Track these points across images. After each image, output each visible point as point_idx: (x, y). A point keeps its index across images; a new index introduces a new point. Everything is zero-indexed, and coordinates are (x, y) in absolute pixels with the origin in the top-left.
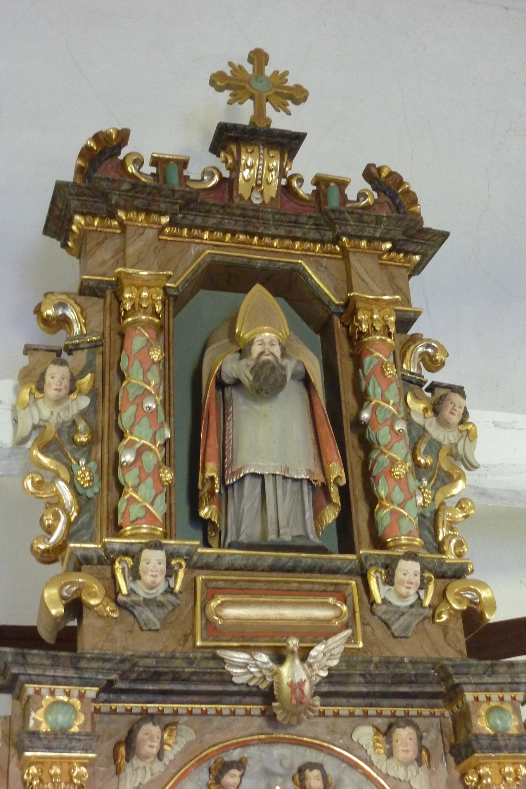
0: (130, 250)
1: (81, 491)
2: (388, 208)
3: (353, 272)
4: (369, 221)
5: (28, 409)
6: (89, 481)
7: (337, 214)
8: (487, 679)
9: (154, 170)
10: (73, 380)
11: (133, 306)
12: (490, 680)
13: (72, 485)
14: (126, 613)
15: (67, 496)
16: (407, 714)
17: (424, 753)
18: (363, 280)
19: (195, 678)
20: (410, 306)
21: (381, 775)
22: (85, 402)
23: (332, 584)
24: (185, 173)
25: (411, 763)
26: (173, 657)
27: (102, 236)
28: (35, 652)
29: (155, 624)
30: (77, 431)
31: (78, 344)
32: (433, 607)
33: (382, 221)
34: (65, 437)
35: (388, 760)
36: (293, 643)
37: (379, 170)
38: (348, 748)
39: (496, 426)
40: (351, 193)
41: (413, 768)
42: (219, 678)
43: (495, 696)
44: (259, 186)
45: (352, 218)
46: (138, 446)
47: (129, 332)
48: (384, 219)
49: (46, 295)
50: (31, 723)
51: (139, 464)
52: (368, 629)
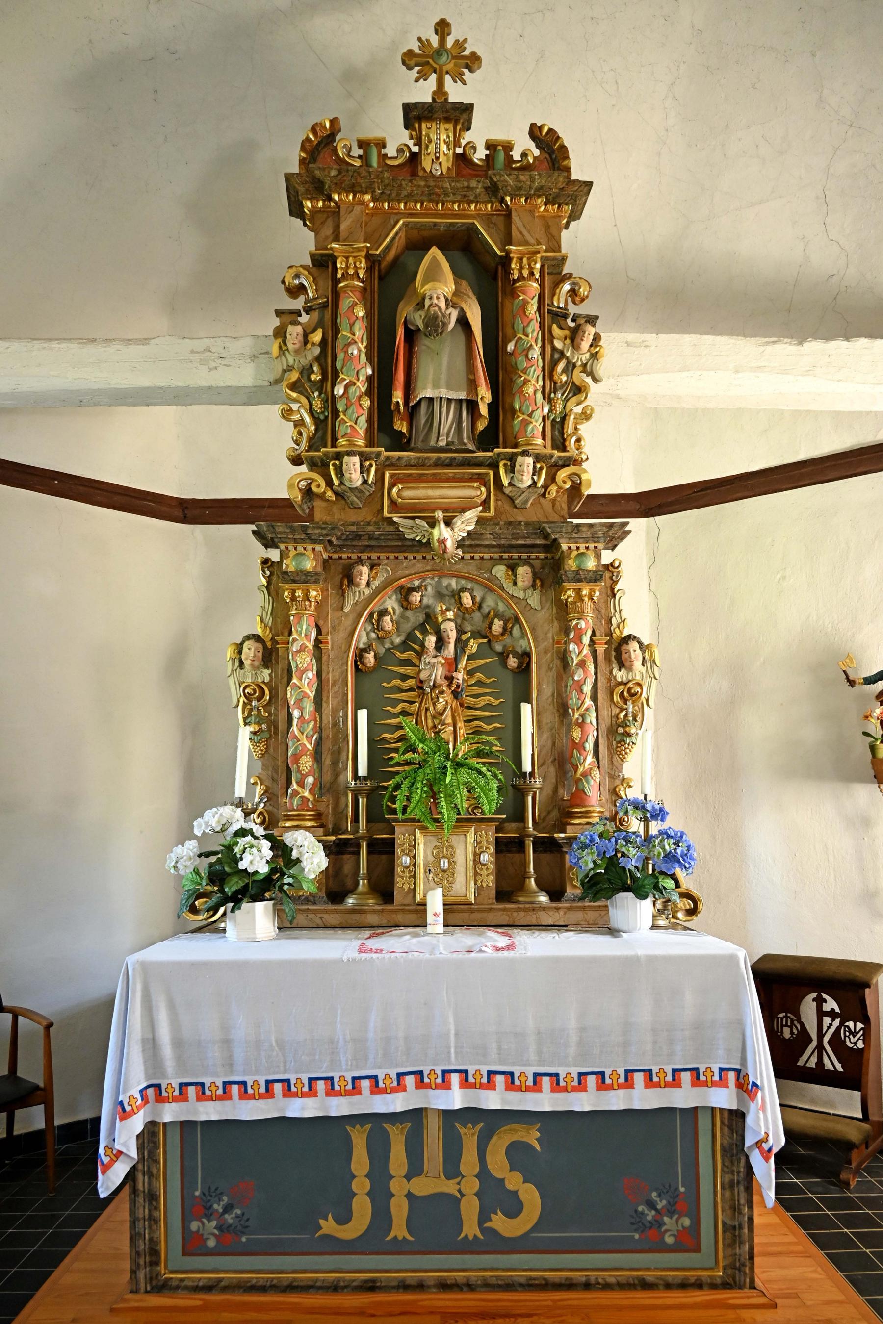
0: (343, 226)
1: (316, 415)
2: (546, 164)
3: (513, 226)
4: (524, 179)
5: (279, 359)
6: (321, 408)
7: (498, 177)
8: (574, 535)
9: (361, 152)
10: (306, 335)
11: (343, 274)
12: (577, 536)
13: (311, 412)
14: (340, 498)
15: (307, 419)
16: (529, 558)
17: (537, 581)
18: (521, 233)
19: (382, 538)
20: (560, 252)
22: (317, 351)
23: (476, 474)
24: (384, 151)
25: (529, 588)
26: (369, 524)
27: (325, 215)
28: (279, 524)
29: (357, 504)
30: (313, 372)
31: (311, 306)
32: (546, 487)
33: (535, 179)
34: (306, 377)
36: (440, 515)
37: (540, 128)
39: (628, 346)
40: (516, 155)
41: (529, 592)
42: (397, 537)
43: (582, 547)
44: (437, 158)
45: (510, 179)
46: (346, 382)
47: (342, 295)
48: (537, 177)
49: (289, 267)
50: (284, 566)
51: (346, 396)
52: (500, 503)
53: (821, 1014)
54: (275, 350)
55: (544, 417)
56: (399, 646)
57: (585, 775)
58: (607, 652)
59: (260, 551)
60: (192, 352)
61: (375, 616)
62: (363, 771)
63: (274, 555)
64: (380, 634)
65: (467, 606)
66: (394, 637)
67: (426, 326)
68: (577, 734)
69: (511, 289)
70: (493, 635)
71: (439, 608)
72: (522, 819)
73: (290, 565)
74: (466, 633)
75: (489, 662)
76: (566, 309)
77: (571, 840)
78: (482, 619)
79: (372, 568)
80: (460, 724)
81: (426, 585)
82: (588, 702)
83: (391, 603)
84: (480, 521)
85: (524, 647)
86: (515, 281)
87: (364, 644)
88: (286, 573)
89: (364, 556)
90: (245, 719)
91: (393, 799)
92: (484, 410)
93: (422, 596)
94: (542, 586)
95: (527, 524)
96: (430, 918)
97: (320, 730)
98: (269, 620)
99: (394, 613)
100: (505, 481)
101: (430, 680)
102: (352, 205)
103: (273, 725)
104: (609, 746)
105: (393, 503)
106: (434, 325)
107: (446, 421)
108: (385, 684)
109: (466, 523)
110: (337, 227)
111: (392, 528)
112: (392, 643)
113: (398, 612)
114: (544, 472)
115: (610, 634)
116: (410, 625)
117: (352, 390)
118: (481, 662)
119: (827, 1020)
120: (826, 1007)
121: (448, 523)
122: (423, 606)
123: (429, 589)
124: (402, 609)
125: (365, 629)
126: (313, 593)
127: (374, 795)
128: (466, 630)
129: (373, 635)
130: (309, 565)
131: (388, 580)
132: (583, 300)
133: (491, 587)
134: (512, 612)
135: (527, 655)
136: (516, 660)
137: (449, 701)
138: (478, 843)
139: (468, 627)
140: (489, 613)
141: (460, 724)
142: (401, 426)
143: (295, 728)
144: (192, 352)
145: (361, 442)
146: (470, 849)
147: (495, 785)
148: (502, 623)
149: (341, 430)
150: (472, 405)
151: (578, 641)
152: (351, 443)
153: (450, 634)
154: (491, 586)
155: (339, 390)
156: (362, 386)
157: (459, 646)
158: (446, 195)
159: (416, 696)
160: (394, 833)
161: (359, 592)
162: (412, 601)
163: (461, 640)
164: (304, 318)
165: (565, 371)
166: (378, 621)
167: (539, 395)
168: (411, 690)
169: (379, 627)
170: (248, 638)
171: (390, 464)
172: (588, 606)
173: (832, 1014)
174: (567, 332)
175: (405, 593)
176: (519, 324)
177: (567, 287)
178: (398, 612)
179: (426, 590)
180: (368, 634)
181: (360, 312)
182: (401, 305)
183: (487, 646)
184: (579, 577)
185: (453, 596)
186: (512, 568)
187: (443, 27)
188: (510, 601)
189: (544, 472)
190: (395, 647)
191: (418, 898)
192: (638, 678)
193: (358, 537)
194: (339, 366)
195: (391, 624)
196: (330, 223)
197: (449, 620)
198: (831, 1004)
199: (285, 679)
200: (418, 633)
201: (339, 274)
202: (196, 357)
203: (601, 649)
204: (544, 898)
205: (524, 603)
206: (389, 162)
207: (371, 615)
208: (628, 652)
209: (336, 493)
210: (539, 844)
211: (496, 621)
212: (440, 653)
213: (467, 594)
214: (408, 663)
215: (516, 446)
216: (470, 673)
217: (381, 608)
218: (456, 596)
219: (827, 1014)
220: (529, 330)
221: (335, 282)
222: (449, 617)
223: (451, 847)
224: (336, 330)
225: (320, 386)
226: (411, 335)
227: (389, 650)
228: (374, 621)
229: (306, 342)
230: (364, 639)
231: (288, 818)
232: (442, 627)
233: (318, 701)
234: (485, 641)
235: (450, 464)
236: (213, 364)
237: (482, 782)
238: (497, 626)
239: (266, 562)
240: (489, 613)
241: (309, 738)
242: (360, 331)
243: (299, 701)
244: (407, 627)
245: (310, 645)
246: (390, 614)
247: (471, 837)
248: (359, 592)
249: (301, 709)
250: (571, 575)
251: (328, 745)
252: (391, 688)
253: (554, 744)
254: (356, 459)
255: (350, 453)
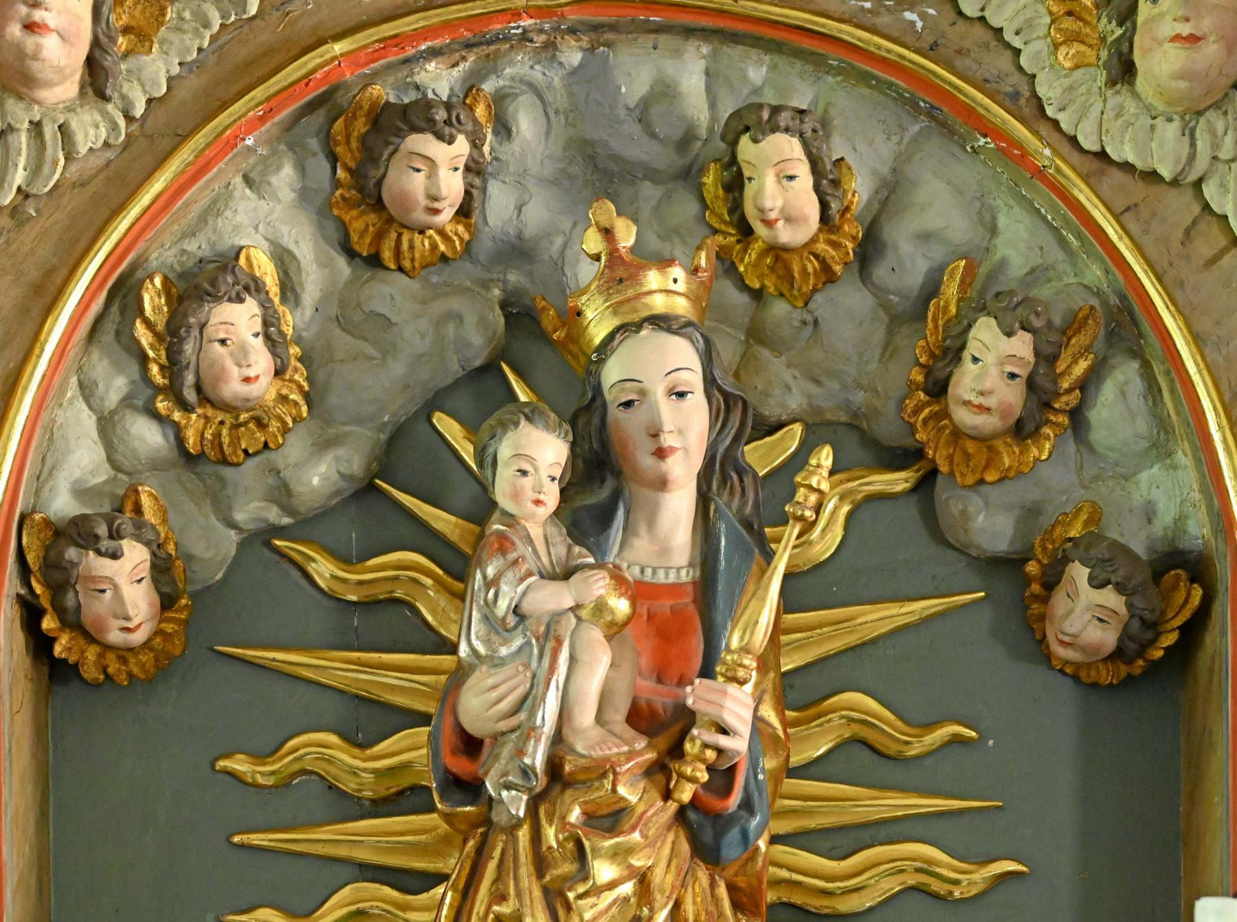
21: (1076, 158)
25: (1216, 106)
35: (1109, 93)
38: (934, 46)
56: (324, 514)
61: (152, 300)
64: (193, 427)
65: (786, 235)
66: (294, 449)
70: (958, 434)
71: (593, 242)
74: (780, 426)
75: (926, 621)
78: (880, 334)
81: (500, 101)
85: (1166, 515)
87: (81, 492)
93: (474, 169)
99: (289, 290)
101: (528, 731)
108: (240, 765)
112: (282, 493)
113: (312, 286)
116: (398, 368)
122: (485, 247)
123: (526, 122)
124: (341, 262)
125: (87, 391)
128: (772, 411)
131: (243, 53)
133: (947, 96)
134: (1095, 273)
136: (1111, 598)
137: (662, 878)
140: (932, 289)
148: (1022, 345)
153: (668, 422)
157: (726, 506)
159: (446, 840)
161: (36, 127)
162: (405, 201)
163: (742, 470)
178: (312, 286)
179: (504, 129)
180: (107, 426)
183: (910, 511)
185: (689, 175)
188: (1083, 195)
195: (262, 362)
197: (662, 322)
200: (447, 425)
205: (1181, 208)
211: (985, 333)
212: (598, 550)
213: (788, 147)
217: (197, 246)
222: (659, 304)
227: (264, 536)
228: (143, 336)
232: (612, 373)
234: (898, 481)
240: (932, 289)
246: (255, 287)
248: (36, 127)
252: (284, 784)
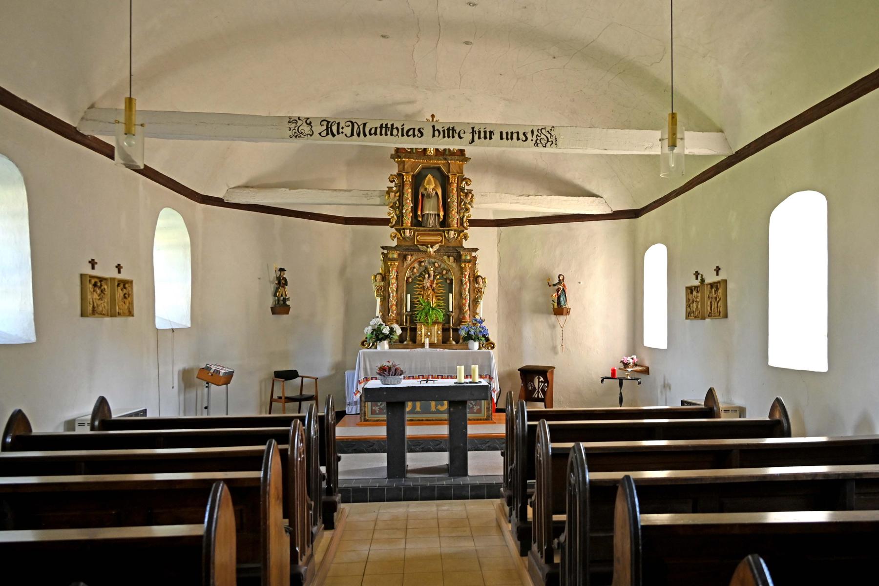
0: (406, 167)
13: (396, 214)
15: (395, 217)
22: (398, 198)
26: (411, 246)
32: (457, 237)
47: (405, 185)
53: (539, 382)
54: (387, 197)
55: (458, 219)
57: (466, 312)
58: (473, 280)
59: (382, 250)
60: (363, 194)
62: (409, 310)
63: (385, 252)
67: (427, 196)
68: (464, 301)
69: (450, 184)
72: (449, 323)
73: (390, 256)
76: (464, 187)
77: (460, 328)
79: (411, 255)
80: (434, 298)
82: (467, 293)
83: (416, 265)
84: (440, 246)
86: (451, 183)
88: (389, 258)
89: (409, 253)
90: (377, 295)
91: (416, 317)
92: (442, 217)
94: (456, 262)
95: (453, 247)
96: (425, 345)
97: (397, 299)
98: (383, 269)
100: (447, 236)
102: (408, 161)
103: (384, 297)
104: (473, 304)
105: (417, 240)
106: (429, 196)
107: (432, 219)
109: (437, 247)
110: (404, 166)
111: (417, 248)
114: (457, 234)
115: (474, 275)
117: (408, 211)
118: (440, 281)
119: (540, 384)
120: (540, 380)
121: (432, 247)
126: (396, 263)
127: (411, 316)
129: (411, 273)
130: (395, 256)
132: (469, 185)
135: (452, 280)
138: (438, 329)
139: (437, 271)
141: (434, 298)
142: (420, 219)
143: (391, 298)
144: (363, 194)
145: (409, 225)
146: (436, 330)
147: (442, 314)
149: (404, 222)
150: (439, 215)
151: (465, 277)
152: (407, 225)
154: (443, 261)
155: (404, 211)
156: (410, 210)
158: (433, 159)
160: (416, 325)
164: (394, 189)
165: (464, 205)
166: (413, 270)
167: (456, 213)
168: (421, 288)
169: (413, 271)
170: (378, 274)
171: (416, 230)
172: (468, 269)
173: (542, 382)
174: (464, 194)
175: (420, 263)
176: (451, 195)
177: (464, 182)
181: (410, 190)
182: (420, 188)
184: (466, 261)
186: (449, 257)
187: (433, 116)
189: (457, 234)
190: (417, 276)
191: (422, 342)
192: (481, 287)
193: (408, 249)
194: (404, 204)
196: (402, 164)
198: (542, 379)
199: (388, 285)
201: (405, 180)
202: (364, 196)
203: (471, 279)
204: (454, 343)
206: (418, 150)
207: (411, 268)
208: (478, 280)
209: (402, 238)
210: (453, 329)
214: (420, 281)
215: (450, 227)
216: (437, 284)
218: (434, 263)
219: (540, 382)
220: (454, 197)
221: (403, 182)
223: (430, 329)
224: (403, 194)
225: (398, 207)
226: (423, 195)
227: (415, 277)
229: (395, 196)
230: (409, 274)
231: (389, 322)
233: (397, 291)
235: (433, 231)
236: (368, 198)
237: (439, 313)
238: (444, 272)
239: (383, 253)
241: (395, 301)
242: (410, 196)
243: (392, 292)
244: (420, 271)
245: (395, 277)
247: (436, 327)
249: (393, 294)
250: (463, 261)
251: (399, 303)
253: (458, 304)
254: (408, 231)
255: (407, 229)
